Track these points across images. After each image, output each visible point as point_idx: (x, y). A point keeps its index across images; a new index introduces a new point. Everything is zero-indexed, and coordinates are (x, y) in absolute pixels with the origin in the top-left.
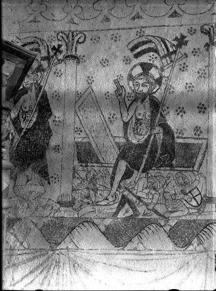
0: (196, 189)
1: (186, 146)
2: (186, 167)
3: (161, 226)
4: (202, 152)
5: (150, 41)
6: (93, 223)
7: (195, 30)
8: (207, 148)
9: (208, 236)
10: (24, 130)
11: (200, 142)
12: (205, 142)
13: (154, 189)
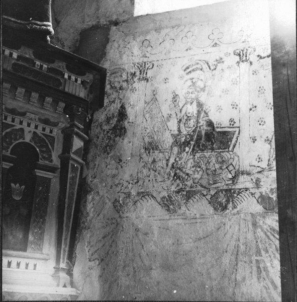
0: (231, 166)
1: (224, 133)
2: (224, 149)
3: (204, 196)
5: (198, 64)
6: (152, 196)
7: (230, 54)
8: (239, 134)
9: (241, 202)
11: (234, 129)
12: (237, 130)
13: (200, 167)
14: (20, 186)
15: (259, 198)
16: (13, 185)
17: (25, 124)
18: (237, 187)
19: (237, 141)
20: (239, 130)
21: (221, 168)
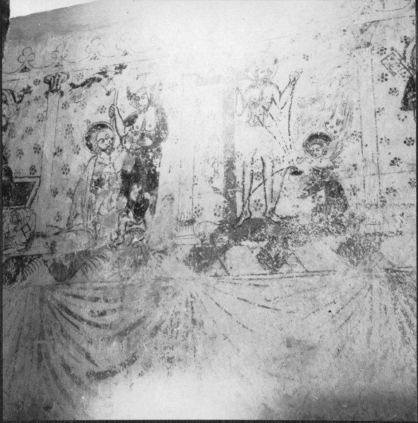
1: (23, 185)
2: (20, 205)
4: (34, 189)
11: (34, 180)
12: (38, 179)
15: (51, 266)
18: (29, 253)
19: (35, 195)
20: (40, 181)
21: (15, 230)
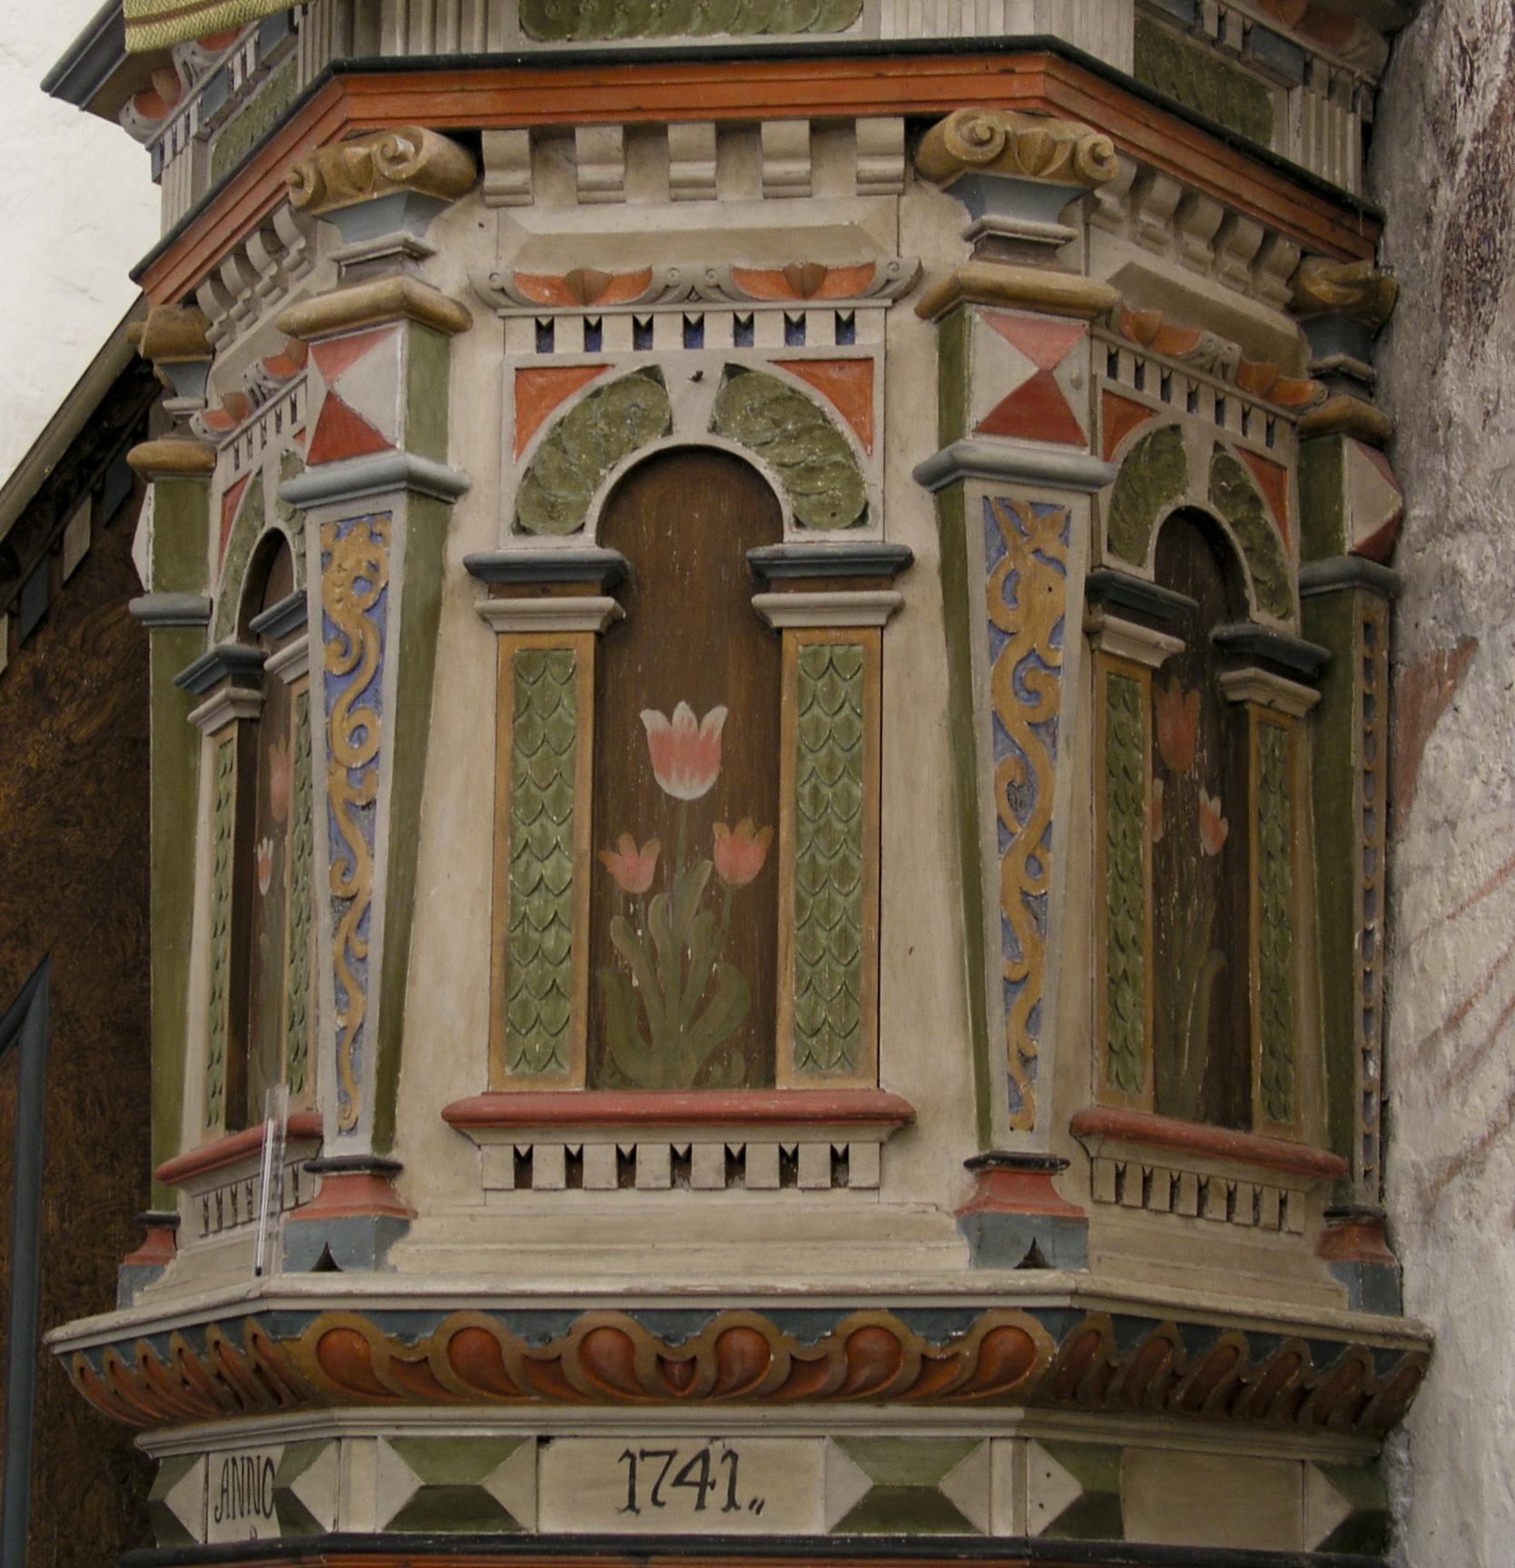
10: (1468, 147)
14: (700, 712)
16: (651, 719)
17: (667, 338)
